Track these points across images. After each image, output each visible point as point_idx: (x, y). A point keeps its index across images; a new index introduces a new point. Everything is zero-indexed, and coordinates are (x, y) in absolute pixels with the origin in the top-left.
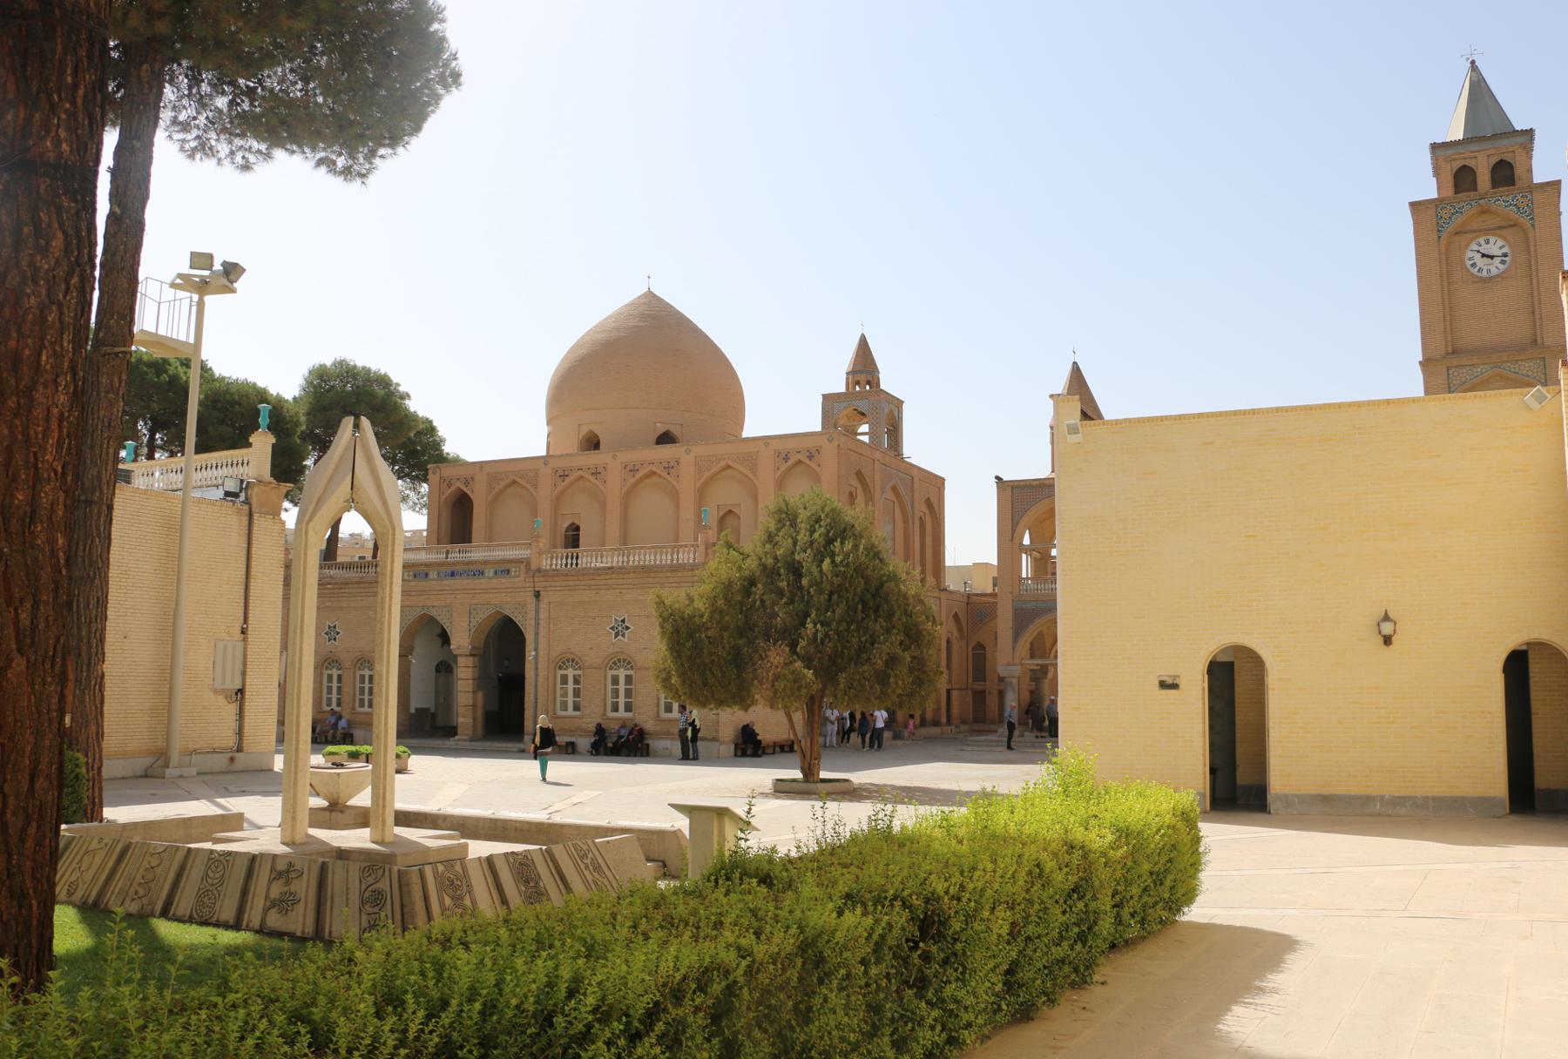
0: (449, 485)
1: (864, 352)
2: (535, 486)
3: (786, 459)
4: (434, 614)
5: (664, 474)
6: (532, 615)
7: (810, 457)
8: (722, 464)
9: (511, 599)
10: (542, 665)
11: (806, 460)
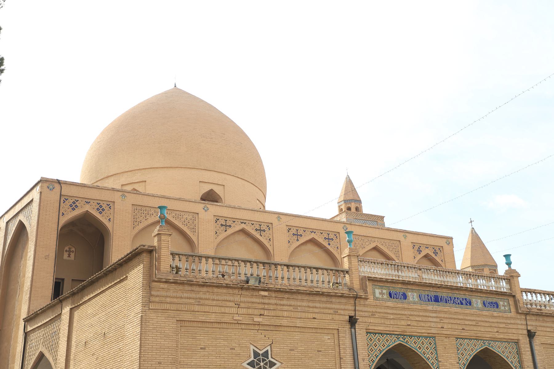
1: (350, 186)
2: (193, 230)
3: (419, 251)
4: (411, 344)
5: (325, 243)
7: (436, 253)
8: (373, 245)
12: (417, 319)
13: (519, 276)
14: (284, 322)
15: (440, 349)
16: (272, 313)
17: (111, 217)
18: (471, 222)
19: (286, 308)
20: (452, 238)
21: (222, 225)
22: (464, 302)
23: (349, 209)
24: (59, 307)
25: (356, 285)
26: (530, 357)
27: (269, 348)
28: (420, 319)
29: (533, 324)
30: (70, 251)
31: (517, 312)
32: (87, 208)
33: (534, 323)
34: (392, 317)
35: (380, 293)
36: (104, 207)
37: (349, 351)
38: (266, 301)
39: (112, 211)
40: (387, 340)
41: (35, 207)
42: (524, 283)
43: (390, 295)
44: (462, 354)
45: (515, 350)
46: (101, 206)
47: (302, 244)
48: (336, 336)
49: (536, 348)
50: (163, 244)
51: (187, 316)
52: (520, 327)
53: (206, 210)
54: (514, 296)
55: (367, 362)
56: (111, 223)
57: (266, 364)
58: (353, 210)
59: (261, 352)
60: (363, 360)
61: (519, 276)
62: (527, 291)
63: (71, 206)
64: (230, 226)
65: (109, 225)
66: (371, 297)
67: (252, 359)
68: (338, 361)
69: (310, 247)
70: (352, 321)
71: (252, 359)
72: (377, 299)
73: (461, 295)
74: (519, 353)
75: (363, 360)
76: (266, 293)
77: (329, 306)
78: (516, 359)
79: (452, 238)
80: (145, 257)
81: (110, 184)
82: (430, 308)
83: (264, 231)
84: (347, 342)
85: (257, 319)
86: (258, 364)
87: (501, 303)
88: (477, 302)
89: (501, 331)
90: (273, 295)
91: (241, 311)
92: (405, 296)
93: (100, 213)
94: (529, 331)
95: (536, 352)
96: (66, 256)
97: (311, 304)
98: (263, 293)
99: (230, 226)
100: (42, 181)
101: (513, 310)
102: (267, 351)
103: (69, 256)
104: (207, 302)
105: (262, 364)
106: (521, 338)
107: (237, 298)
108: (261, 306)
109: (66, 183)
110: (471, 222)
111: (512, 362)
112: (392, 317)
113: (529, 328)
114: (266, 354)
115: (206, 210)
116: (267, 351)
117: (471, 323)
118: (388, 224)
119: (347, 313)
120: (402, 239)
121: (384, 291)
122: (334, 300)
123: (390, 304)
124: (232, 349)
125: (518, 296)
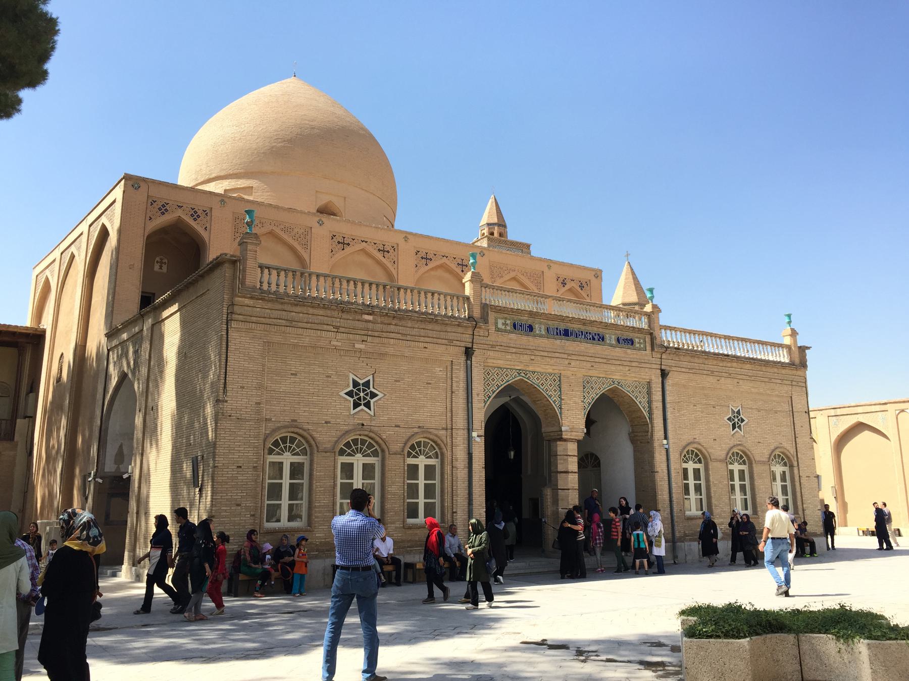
0: (163, 210)
2: (306, 246)
3: (564, 284)
4: (534, 380)
6: (657, 396)
7: (582, 287)
8: (512, 275)
9: (629, 374)
10: (674, 456)
11: (579, 289)
12: (542, 354)
13: (660, 311)
14: (390, 350)
15: (564, 387)
16: (377, 340)
17: (208, 225)
18: (628, 255)
19: (392, 335)
20: (601, 271)
21: (339, 243)
22: (596, 337)
23: (492, 234)
24: (140, 322)
25: (477, 313)
26: (660, 398)
27: (371, 378)
28: (546, 354)
29: (668, 362)
30: (161, 263)
31: (653, 349)
32: (179, 213)
33: (670, 362)
34: (514, 350)
35: (503, 324)
36: (199, 213)
37: (462, 385)
38: (370, 326)
39: (208, 218)
40: (507, 376)
41: (118, 207)
42: (664, 319)
43: (514, 326)
44: (588, 393)
45: (645, 390)
46: (195, 212)
47: (432, 269)
48: (449, 368)
49: (668, 388)
50: (250, 255)
51: (277, 338)
52: (654, 366)
53: (321, 223)
54: (651, 334)
55: (482, 397)
56: (208, 232)
57: (367, 394)
58: (496, 235)
59: (361, 382)
60: (478, 395)
61: (660, 311)
62: (667, 328)
63: (160, 209)
64: (348, 244)
65: (204, 234)
66: (492, 328)
67: (351, 388)
68: (449, 395)
69: (440, 272)
70: (469, 352)
71: (351, 388)
72: (498, 330)
73: (595, 330)
74: (649, 393)
75: (478, 395)
76: (370, 318)
77: (443, 335)
78: (646, 399)
79: (601, 271)
80: (227, 270)
81: (211, 187)
82: (558, 342)
83: (388, 252)
84: (462, 375)
85: (357, 346)
86: (357, 394)
87: (637, 340)
88: (611, 338)
89: (633, 369)
90: (379, 320)
91: (339, 336)
92: (531, 328)
93: (195, 220)
94: (662, 371)
95: (667, 393)
96: (157, 267)
97: (423, 332)
98: (367, 317)
99: (348, 244)
100: (127, 178)
101: (649, 348)
102: (369, 381)
103: (161, 268)
104: (300, 324)
105: (362, 394)
106: (653, 378)
107: (337, 322)
108: (363, 332)
109: (154, 182)
110: (628, 255)
111: (640, 402)
112: (514, 350)
113: (663, 367)
114: (367, 384)
115: (321, 223)
116: (369, 381)
117: (601, 360)
118: (535, 252)
119: (463, 344)
120: (546, 270)
121: (508, 322)
122: (449, 329)
123: (513, 336)
124: (328, 377)
125: (656, 333)
